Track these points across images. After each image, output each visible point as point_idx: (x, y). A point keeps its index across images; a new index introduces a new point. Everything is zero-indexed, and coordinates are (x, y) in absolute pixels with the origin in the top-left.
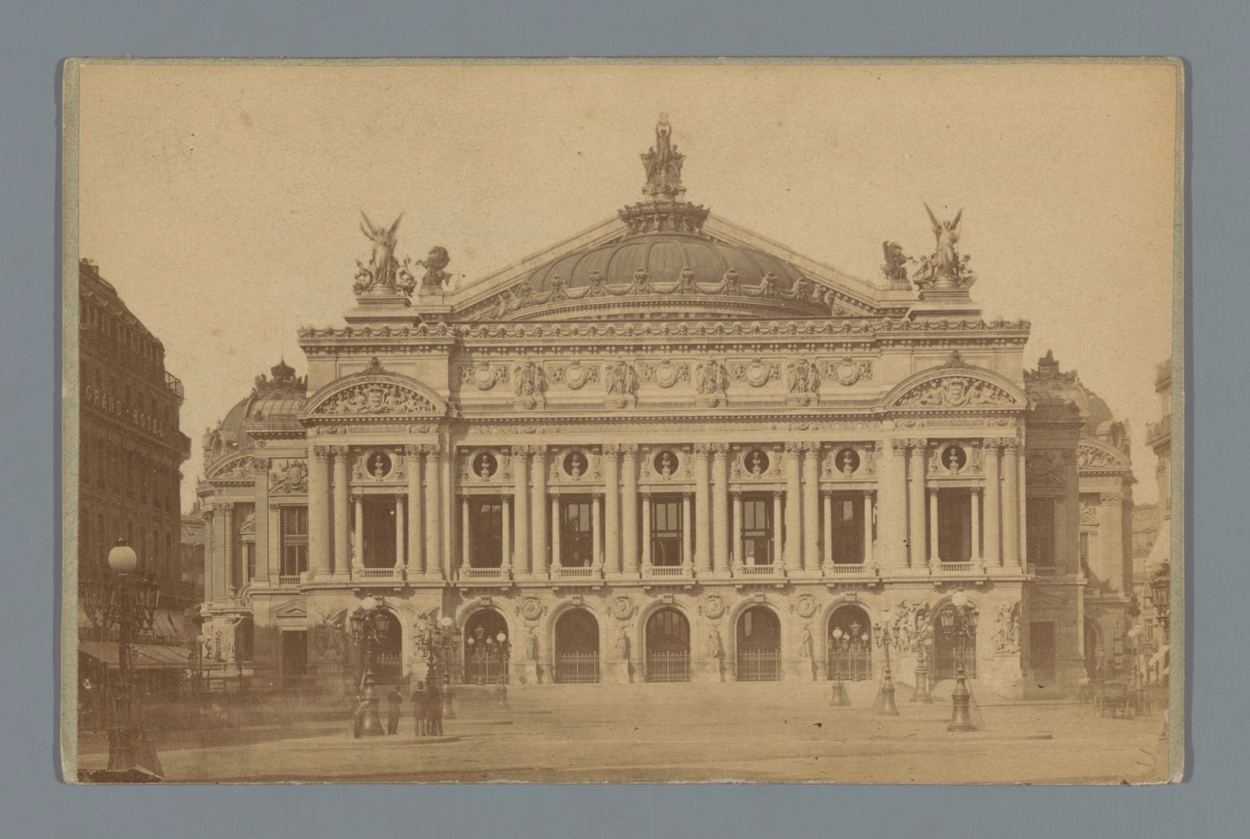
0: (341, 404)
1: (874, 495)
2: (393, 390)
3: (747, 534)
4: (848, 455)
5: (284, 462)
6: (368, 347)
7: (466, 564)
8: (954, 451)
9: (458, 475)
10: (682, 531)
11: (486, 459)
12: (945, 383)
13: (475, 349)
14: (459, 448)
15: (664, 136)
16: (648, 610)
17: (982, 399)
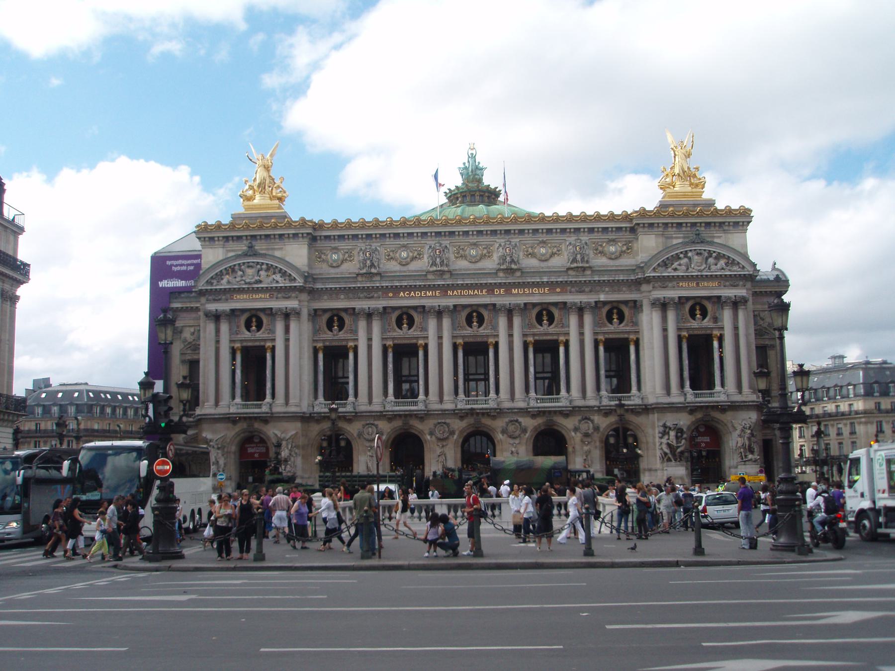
0: (226, 278)
1: (637, 343)
2: (264, 267)
3: (538, 375)
4: (614, 312)
5: (192, 330)
6: (246, 236)
7: (321, 399)
8: (698, 307)
9: (316, 331)
10: (488, 374)
11: (336, 320)
12: (690, 254)
13: (327, 237)
14: (316, 310)
15: (473, 157)
16: (461, 432)
17: (719, 266)
